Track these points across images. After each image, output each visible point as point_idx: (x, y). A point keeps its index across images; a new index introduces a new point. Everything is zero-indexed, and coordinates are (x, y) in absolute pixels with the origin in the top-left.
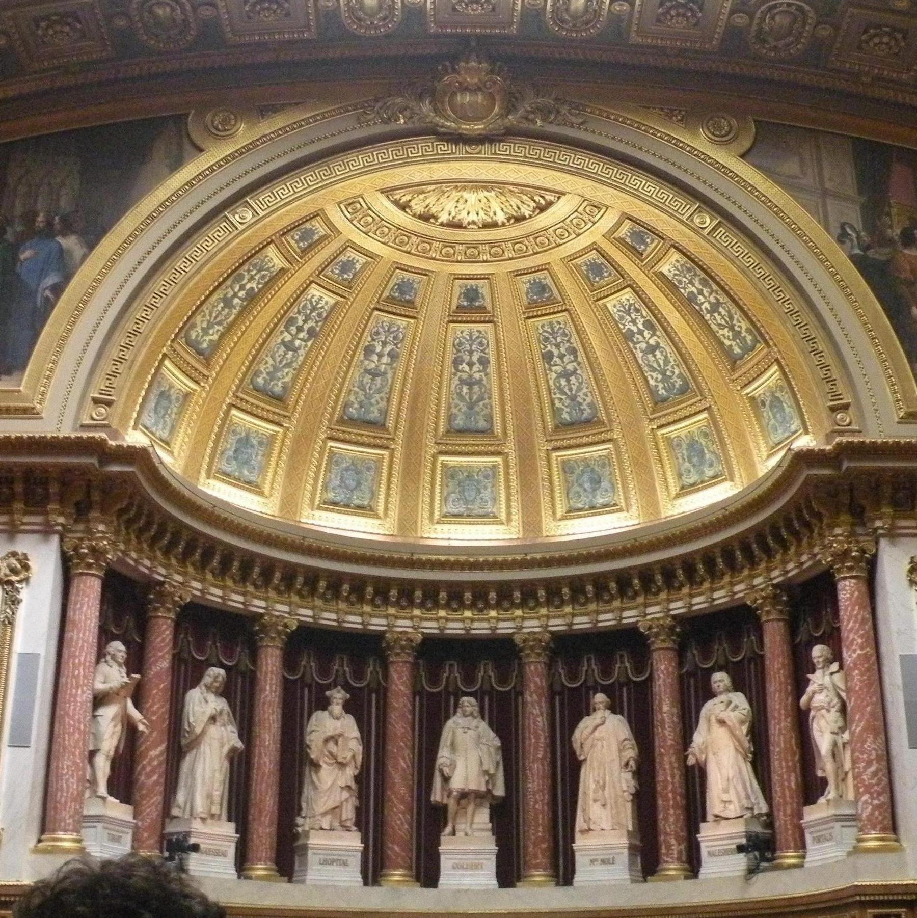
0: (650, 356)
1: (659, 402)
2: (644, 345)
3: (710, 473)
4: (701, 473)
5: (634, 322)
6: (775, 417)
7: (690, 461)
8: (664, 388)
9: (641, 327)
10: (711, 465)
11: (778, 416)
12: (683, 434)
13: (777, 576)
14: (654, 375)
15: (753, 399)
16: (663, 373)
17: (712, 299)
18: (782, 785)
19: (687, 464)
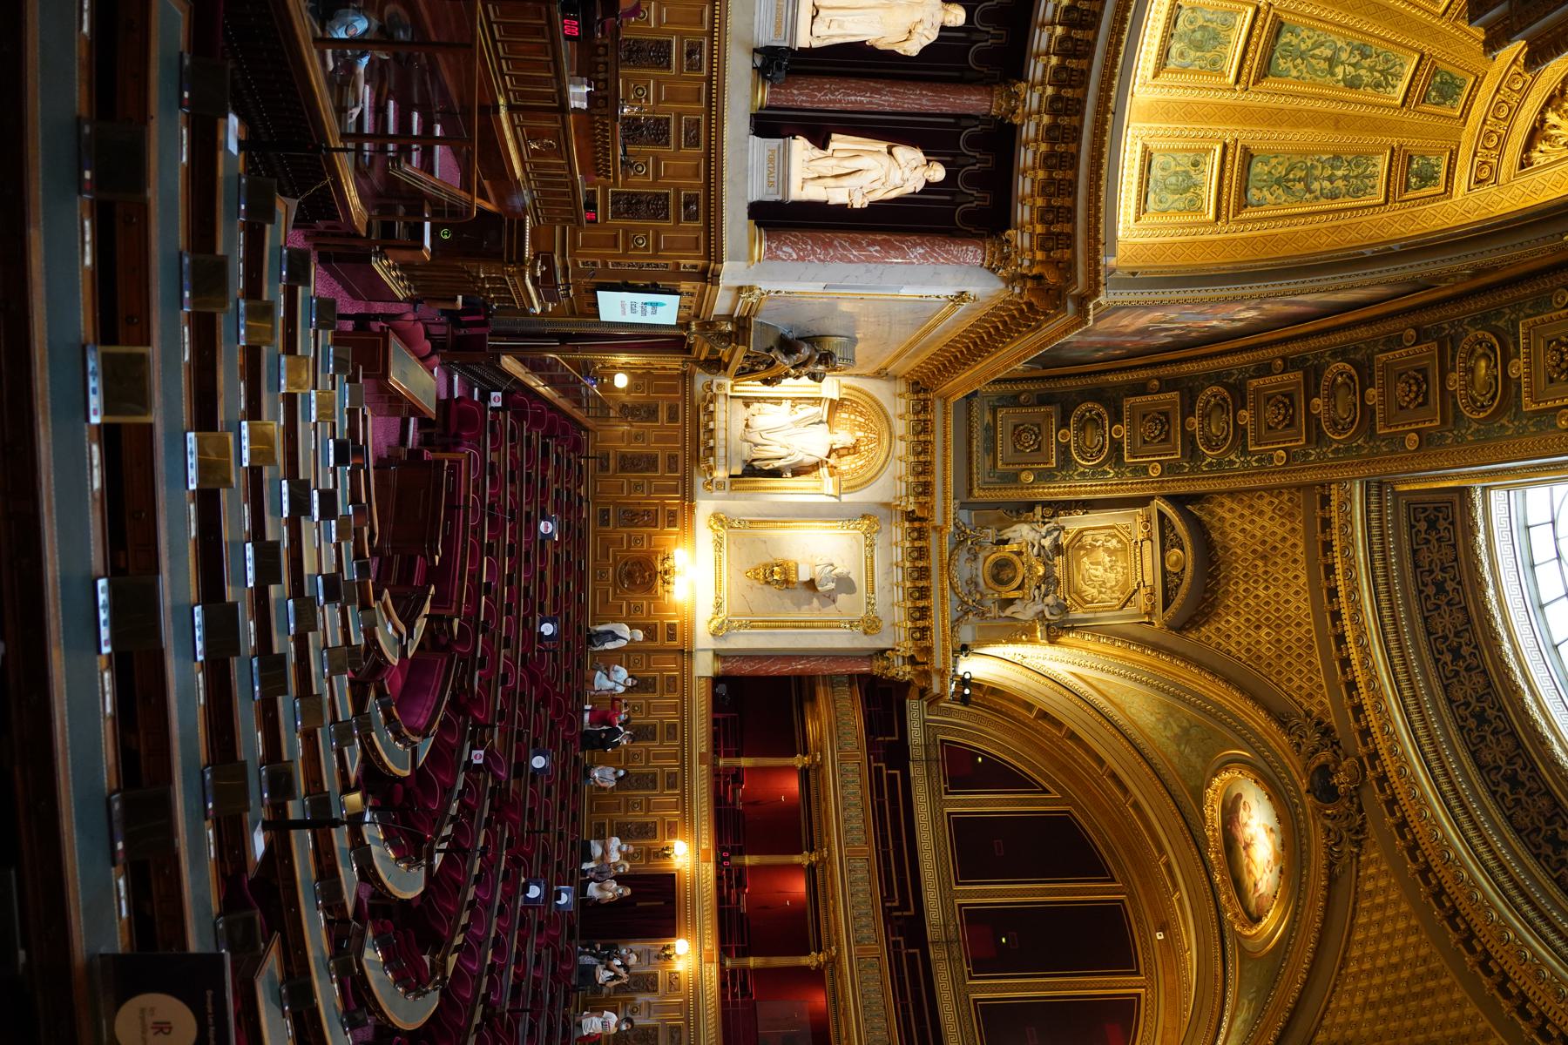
0: (1328, 53)
1: (1278, 27)
2: (1344, 56)
3: (1173, 52)
4: (1180, 39)
5: (1371, 69)
6: (1176, 173)
7: (1202, 27)
8: (1289, 44)
9: (1363, 72)
10: (1182, 54)
11: (1173, 179)
12: (1233, 38)
13: (1029, 130)
14: (1309, 43)
15: (1207, 151)
16: (1302, 55)
17: (1316, 186)
18: (831, 101)
19: (1200, 22)
